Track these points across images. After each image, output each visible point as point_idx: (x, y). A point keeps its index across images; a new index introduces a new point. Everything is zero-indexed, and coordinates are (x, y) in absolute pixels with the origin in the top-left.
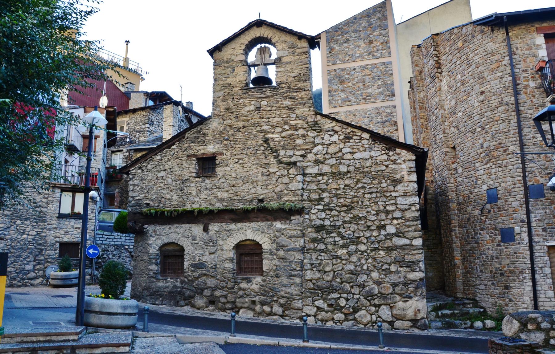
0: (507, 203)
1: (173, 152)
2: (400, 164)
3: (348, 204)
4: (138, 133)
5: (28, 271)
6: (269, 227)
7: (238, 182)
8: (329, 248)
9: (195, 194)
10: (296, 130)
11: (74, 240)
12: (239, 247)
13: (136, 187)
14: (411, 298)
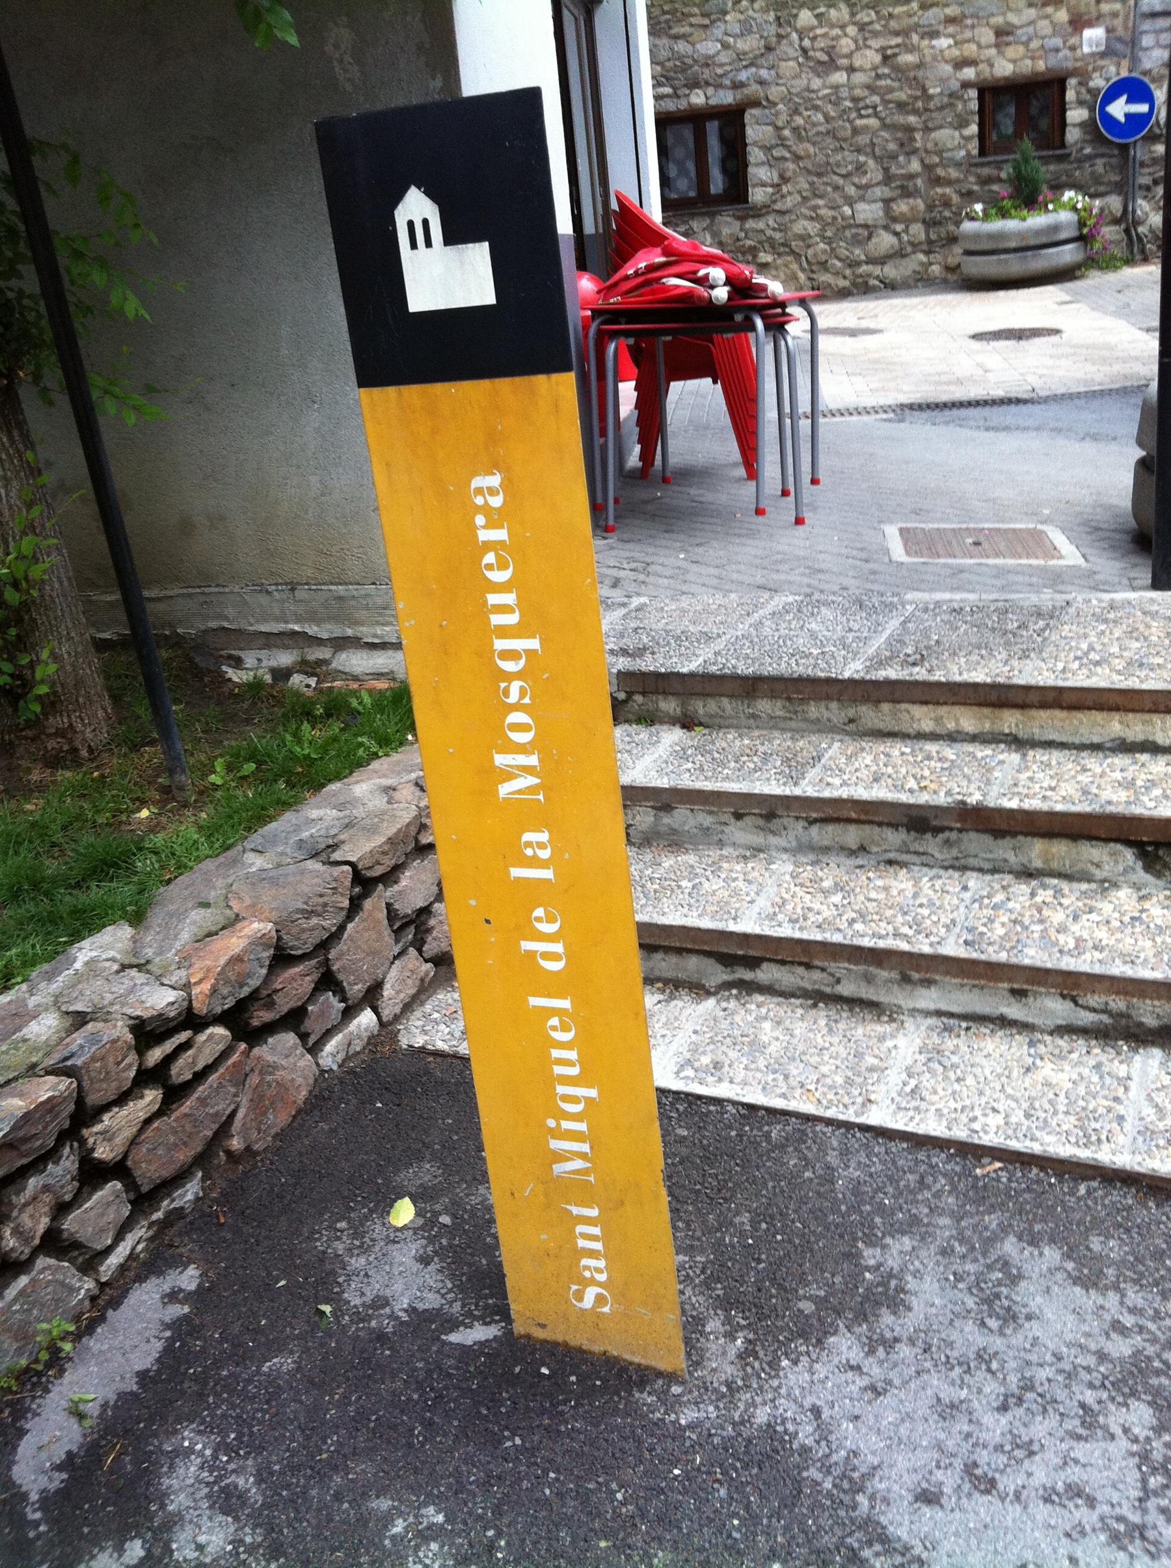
5: (866, 226)
11: (1041, 66)
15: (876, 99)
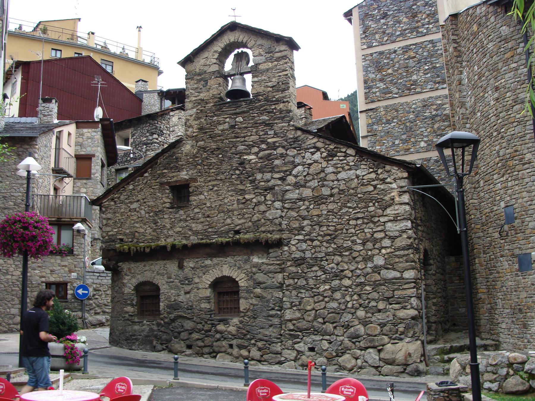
0: (524, 224)
1: (146, 181)
2: (391, 183)
3: (330, 232)
4: (145, 146)
6: (247, 261)
7: (213, 212)
9: (169, 227)
10: (275, 150)
11: (61, 280)
12: (216, 284)
13: (109, 221)
14: (401, 339)
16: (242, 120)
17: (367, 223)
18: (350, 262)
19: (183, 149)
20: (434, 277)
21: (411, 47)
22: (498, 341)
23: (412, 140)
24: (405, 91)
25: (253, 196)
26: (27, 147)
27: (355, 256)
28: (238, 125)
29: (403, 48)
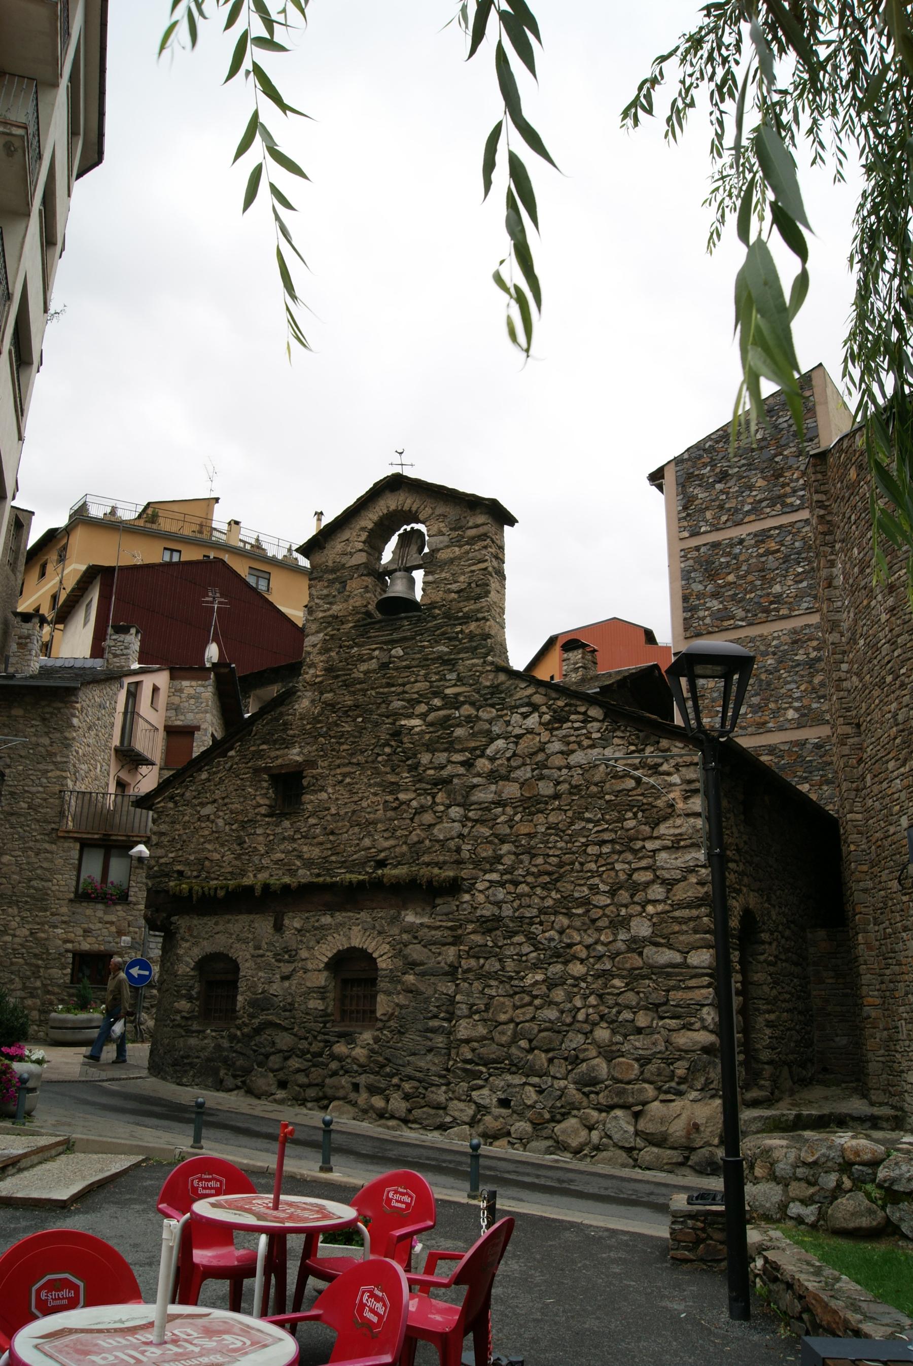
1: (229, 764)
2: (669, 774)
3: (550, 868)
6: (394, 920)
7: (340, 824)
8: (508, 969)
9: (263, 852)
10: (457, 709)
11: (102, 948)
13: (163, 838)
14: (680, 1094)
15: (24, 950)
16: (401, 653)
17: (620, 853)
18: (585, 927)
19: (296, 707)
20: (772, 969)
21: (772, 532)
22: (901, 1109)
23: (772, 706)
24: (760, 615)
25: (412, 795)
26: (60, 705)
27: (594, 917)
28: (394, 662)
29: (755, 535)
